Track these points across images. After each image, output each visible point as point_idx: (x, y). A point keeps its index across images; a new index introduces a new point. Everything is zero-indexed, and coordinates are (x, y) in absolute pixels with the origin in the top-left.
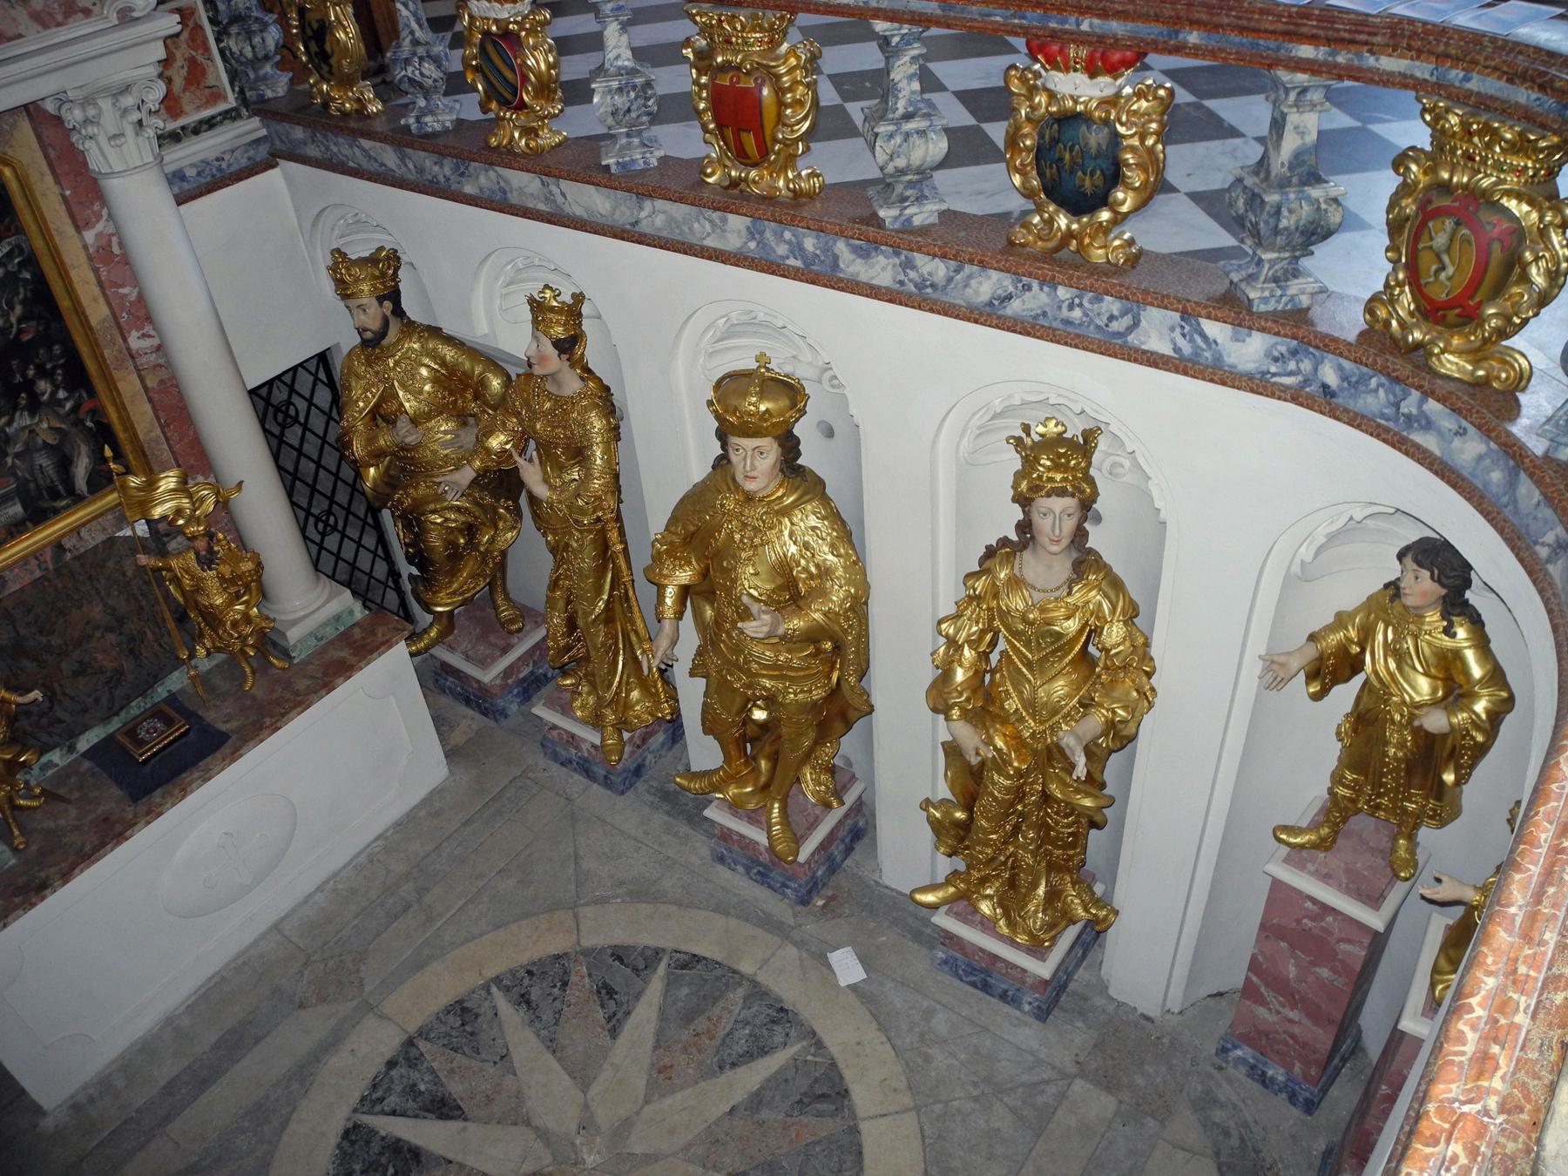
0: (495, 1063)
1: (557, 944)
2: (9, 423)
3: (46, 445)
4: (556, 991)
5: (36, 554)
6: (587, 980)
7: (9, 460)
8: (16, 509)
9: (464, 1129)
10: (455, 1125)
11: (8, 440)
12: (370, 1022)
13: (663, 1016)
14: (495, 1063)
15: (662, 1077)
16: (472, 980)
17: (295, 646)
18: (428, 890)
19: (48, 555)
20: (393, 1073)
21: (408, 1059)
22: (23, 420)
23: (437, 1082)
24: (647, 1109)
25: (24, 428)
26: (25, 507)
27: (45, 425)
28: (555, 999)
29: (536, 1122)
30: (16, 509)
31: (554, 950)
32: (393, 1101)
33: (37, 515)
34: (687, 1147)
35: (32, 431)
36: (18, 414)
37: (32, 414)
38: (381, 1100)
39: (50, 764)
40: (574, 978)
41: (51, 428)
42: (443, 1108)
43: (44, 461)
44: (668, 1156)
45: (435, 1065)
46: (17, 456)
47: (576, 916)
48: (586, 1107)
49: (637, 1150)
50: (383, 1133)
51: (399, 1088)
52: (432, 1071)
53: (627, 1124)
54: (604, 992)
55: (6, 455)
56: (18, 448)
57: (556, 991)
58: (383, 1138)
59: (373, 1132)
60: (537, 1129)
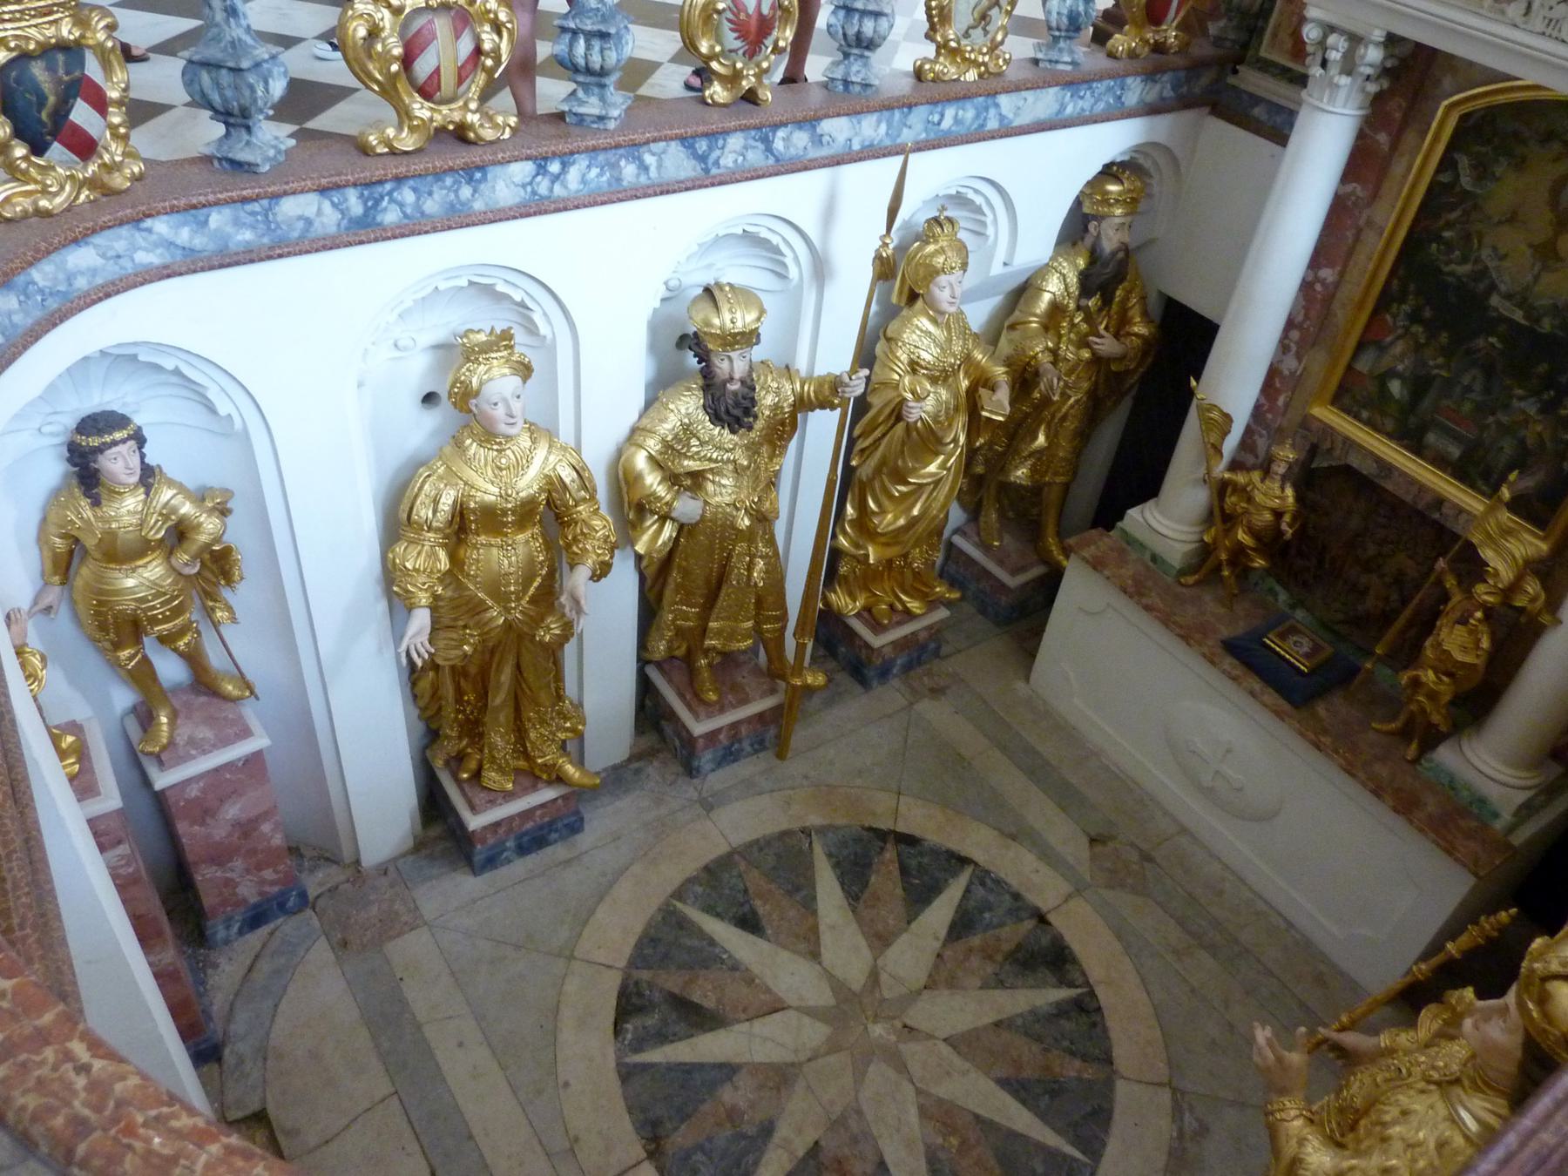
0: (996, 974)
1: (1123, 1053)
2: (1521, 399)
3: (1522, 442)
4: (1066, 1043)
5: (1422, 488)
6: (1073, 1074)
7: (1491, 419)
8: (1455, 451)
9: (937, 939)
10: (943, 933)
11: (1506, 407)
12: (1065, 888)
13: (1013, 1135)
14: (996, 974)
15: (940, 1114)
16: (1095, 972)
17: (1431, 761)
18: (1214, 956)
19: (1428, 498)
20: (1007, 897)
21: (1018, 909)
22: (1531, 407)
23: (989, 926)
24: (909, 1091)
25: (1524, 412)
26: (1461, 458)
27: (1539, 428)
28: (1056, 1040)
29: (926, 994)
30: (1455, 451)
31: (1118, 1053)
32: (980, 892)
33: (1461, 471)
34: (859, 1112)
35: (1526, 422)
36: (1532, 400)
37: (1542, 411)
38: (983, 884)
39: (1275, 595)
40: (1077, 1063)
41: (1540, 435)
42: (962, 926)
43: (1508, 446)
44: (857, 1092)
45: (1007, 929)
46: (1499, 423)
47: (1160, 1084)
48: (930, 1037)
49: (872, 1068)
50: (951, 881)
51: (991, 898)
52: (1001, 925)
53: (902, 1067)
54: (1056, 1086)
55: (1493, 414)
56: (1505, 419)
57: (1066, 1043)
58: (946, 880)
59: (955, 874)
60: (919, 993)
